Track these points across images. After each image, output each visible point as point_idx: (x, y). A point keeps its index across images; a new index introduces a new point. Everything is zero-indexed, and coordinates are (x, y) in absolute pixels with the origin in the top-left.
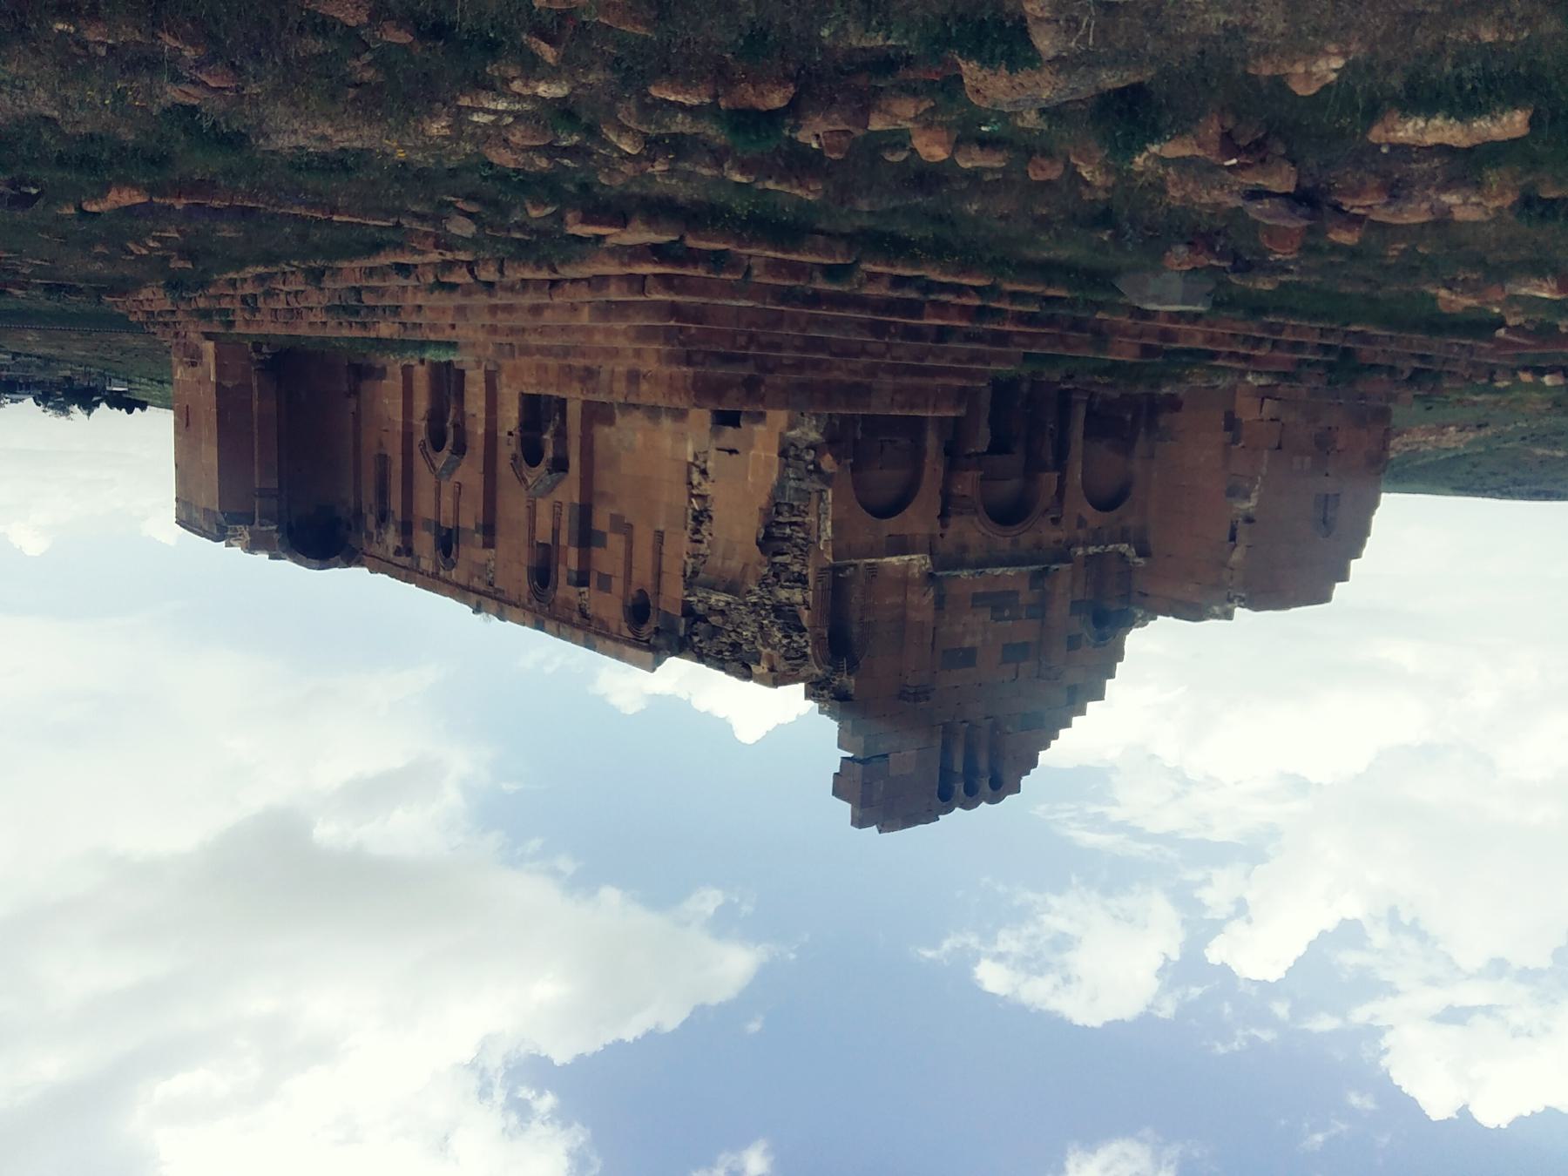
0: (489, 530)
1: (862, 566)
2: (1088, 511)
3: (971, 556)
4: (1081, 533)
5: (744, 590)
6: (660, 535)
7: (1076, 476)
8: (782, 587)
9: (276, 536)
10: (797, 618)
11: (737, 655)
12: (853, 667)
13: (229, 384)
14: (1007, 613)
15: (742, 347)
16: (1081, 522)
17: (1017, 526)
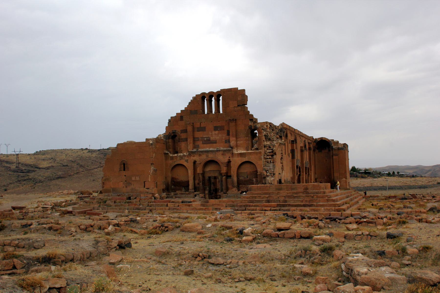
0: (302, 151)
1: (250, 150)
2: (185, 164)
3: (221, 153)
4: (186, 158)
5: (278, 144)
6: (285, 154)
7: (190, 172)
8: (268, 145)
9: (333, 145)
10: (265, 138)
11: (272, 128)
12: (250, 127)
13: (344, 179)
14: (205, 139)
15: (315, 195)
16: (187, 161)
17: (209, 160)
